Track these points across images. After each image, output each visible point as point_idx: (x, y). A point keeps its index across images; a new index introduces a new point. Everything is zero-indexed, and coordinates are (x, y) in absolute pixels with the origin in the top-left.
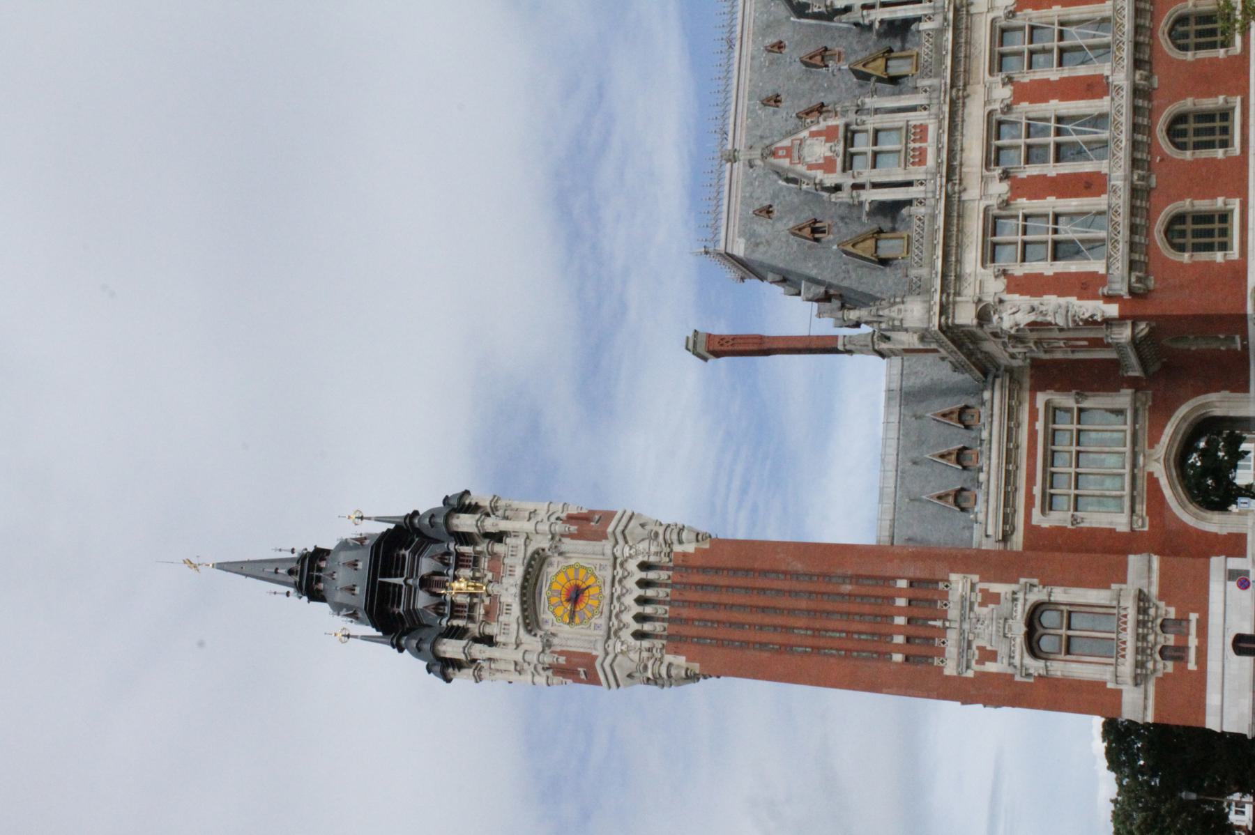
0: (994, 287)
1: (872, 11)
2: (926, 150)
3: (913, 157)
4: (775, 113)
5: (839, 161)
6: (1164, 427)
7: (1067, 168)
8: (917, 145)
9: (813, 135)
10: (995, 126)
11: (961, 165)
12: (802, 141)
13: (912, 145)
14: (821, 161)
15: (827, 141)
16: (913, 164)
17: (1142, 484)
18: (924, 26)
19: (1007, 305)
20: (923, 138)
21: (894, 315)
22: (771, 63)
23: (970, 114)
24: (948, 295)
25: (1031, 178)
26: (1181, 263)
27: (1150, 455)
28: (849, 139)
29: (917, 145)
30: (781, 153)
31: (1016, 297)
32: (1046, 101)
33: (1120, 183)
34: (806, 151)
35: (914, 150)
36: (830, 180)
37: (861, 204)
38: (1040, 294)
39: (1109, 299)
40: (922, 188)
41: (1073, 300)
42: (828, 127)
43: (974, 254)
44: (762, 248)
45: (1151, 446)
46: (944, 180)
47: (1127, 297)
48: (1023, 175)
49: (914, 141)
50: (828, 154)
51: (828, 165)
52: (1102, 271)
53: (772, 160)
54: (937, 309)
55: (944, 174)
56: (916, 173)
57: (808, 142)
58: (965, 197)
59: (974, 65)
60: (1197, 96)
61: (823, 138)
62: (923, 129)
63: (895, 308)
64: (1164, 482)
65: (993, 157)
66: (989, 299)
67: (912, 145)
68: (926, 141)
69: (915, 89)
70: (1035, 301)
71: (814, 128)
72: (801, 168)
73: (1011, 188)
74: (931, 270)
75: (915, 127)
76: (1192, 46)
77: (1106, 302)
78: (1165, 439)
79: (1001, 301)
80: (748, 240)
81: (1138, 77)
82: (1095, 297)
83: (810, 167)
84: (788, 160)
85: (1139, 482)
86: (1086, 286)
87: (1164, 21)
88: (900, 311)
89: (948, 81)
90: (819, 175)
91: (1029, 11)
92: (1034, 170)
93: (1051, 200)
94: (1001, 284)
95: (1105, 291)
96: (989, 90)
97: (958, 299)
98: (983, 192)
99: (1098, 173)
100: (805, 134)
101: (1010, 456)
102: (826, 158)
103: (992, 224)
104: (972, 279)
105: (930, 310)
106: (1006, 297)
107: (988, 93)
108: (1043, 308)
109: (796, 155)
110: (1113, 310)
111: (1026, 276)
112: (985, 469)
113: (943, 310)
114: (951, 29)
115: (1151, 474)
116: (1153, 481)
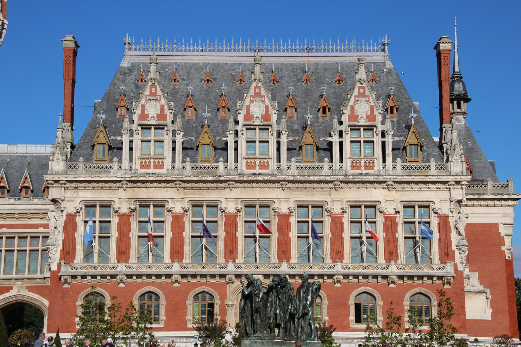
0: (70, 208)
1: (233, 135)
2: (150, 169)
3: (145, 162)
4: (201, 80)
5: (146, 122)
6: (37, 293)
7: (134, 242)
8: (152, 164)
9: (162, 107)
10: (160, 205)
11: (139, 188)
12: (159, 101)
13: (152, 161)
14: (146, 112)
15: (158, 115)
16: (142, 162)
17: (6, 284)
18: (221, 165)
19: (60, 213)
20: (156, 167)
21: (56, 156)
22: (233, 77)
23: (166, 191)
24: (65, 184)
25: (130, 224)
26: (77, 300)
27: (22, 287)
28: (158, 127)
29: (152, 164)
30: (153, 90)
31: (64, 218)
32: (172, 230)
33: (119, 269)
34: (153, 103)
35: (150, 162)
36: (136, 117)
37: (121, 135)
38: (65, 230)
39: (59, 265)
40: (127, 167)
41: (61, 247)
42: (166, 115)
43: (89, 196)
44: (121, 77)
45: (27, 288)
46: (128, 179)
47: (60, 274)
48: (131, 219)
49: (155, 162)
50: (150, 116)
51: (144, 116)
52: (75, 261)
53: (150, 84)
54: (56, 178)
55: (131, 179)
56: (136, 165)
57: (158, 104)
58: (121, 190)
59: (197, 192)
60: (166, 306)
61: (159, 113)
62: (162, 167)
63: (60, 156)
64: (7, 295)
65: (144, 205)
66: (63, 205)
67: (152, 161)
68: (154, 168)
69: (183, 161)
70: (61, 228)
71: (166, 107)
72: (143, 101)
73: (124, 215)
74: (81, 173)
75: (163, 162)
76: (157, 303)
77: (58, 264)
78: (31, 294)
79: (62, 211)
80: (128, 68)
81: (176, 276)
82: (60, 260)
83: (143, 107)
84: (148, 93)
85: (7, 282)
86: (68, 255)
87: (210, 289)
88: (58, 159)
89: (184, 179)
90: (138, 112)
91: (224, 220)
92: (134, 225)
93: (117, 235)
94: (72, 211)
95: (63, 264)
96: (182, 200)
97: (63, 189)
98: (122, 200)
99: (129, 258)
100: (163, 102)
101: (23, 214)
102: (148, 115)
103: (106, 206)
104: (75, 195)
105: (57, 173)
106: (64, 213)
107: (177, 201)
108: (56, 232)
109: (151, 98)
110: (54, 268)
111: (76, 223)
112: (19, 202)
113: (57, 181)
114: (215, 179)
115: (11, 288)
116: (8, 289)
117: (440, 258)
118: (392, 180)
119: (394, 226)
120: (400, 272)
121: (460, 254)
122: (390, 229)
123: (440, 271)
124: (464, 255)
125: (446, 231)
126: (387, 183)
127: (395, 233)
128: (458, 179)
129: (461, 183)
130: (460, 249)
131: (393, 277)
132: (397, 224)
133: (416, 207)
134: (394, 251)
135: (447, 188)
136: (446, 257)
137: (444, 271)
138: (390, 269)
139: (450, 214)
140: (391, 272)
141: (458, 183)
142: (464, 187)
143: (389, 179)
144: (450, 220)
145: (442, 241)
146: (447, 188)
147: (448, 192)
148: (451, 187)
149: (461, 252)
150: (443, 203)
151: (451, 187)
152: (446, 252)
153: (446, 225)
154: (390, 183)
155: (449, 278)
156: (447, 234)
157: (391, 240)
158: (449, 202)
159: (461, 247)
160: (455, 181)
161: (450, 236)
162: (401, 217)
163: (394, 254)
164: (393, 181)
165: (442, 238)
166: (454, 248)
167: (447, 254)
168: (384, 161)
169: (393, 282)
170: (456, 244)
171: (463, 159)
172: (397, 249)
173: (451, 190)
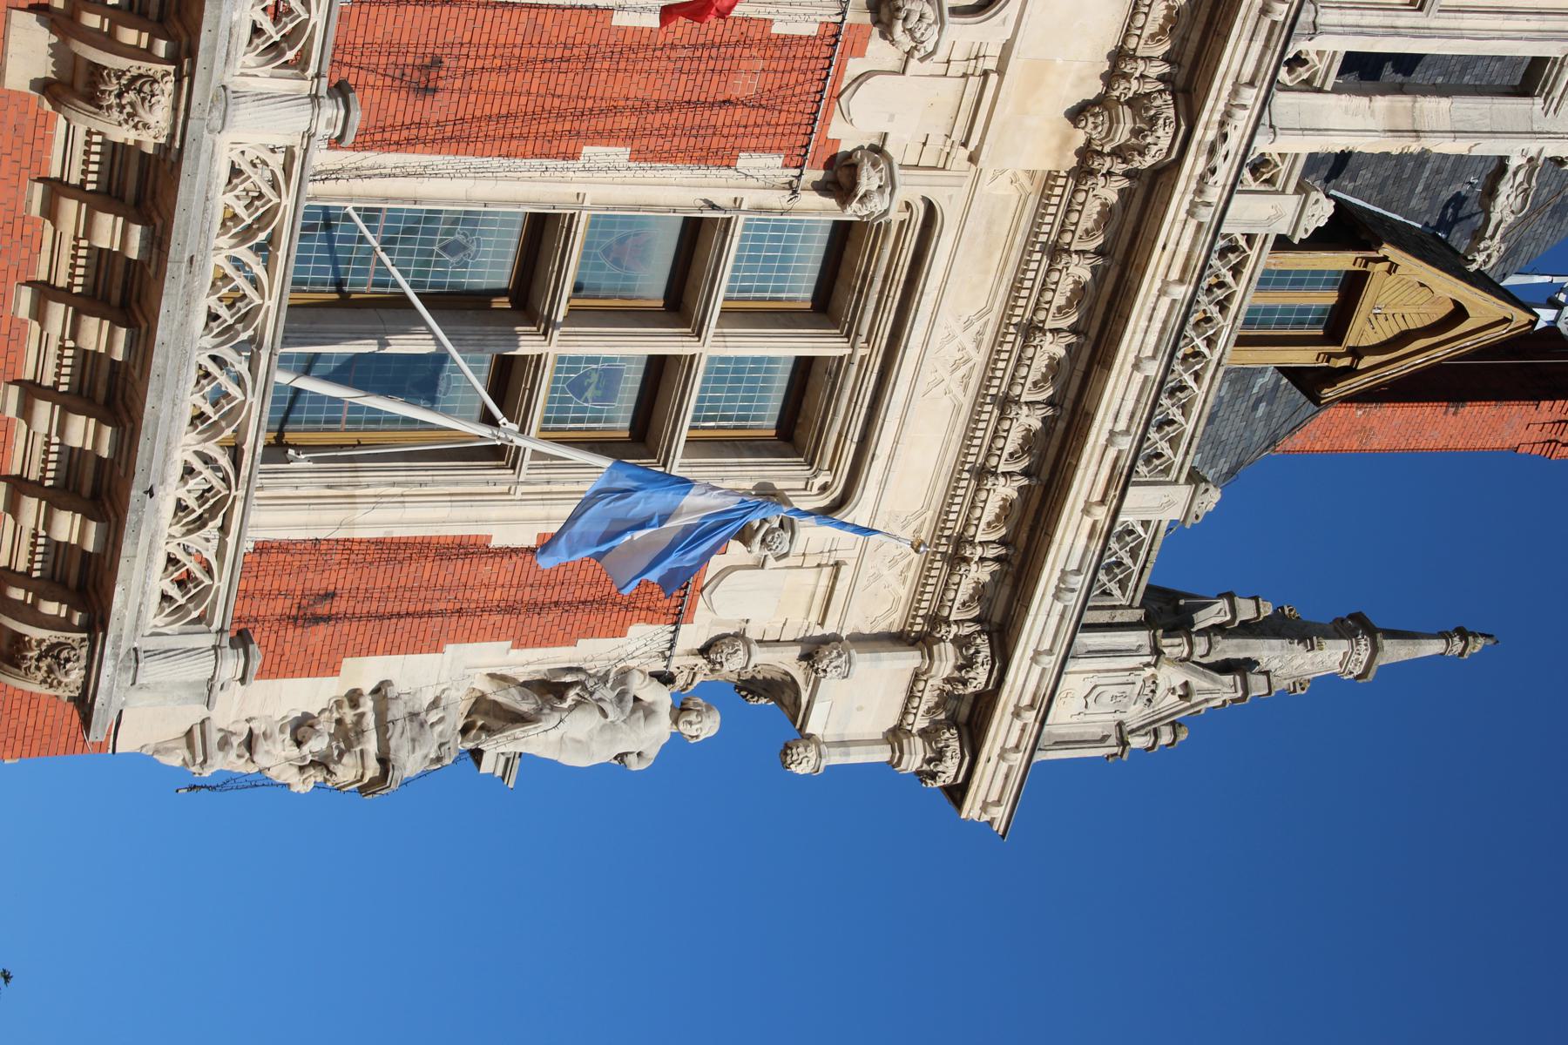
117: (284, 547)
118: (1194, 164)
119: (695, 132)
120: (206, 200)
121: (301, 728)
122: (681, 87)
123: (160, 582)
124: (278, 759)
125: (537, 608)
126: (1165, 106)
127: (629, 137)
128: (1002, 730)
129: (951, 741)
130: (347, 736)
131: (159, 116)
132: (725, 159)
133: (824, 346)
134: (439, 108)
135: (935, 620)
136: (280, 606)
137: (154, 619)
138: (267, 80)
139: (693, 635)
140: (226, 97)
141: (969, 718)
142: (914, 759)
143: (1205, 132)
144: (641, 642)
145: (458, 569)
146: (935, 620)
147: (892, 620)
148: (946, 661)
149: (317, 745)
150: (813, 582)
151: (946, 661)
152: (340, 606)
153: (600, 603)
154: (1162, 140)
155: (76, 675)
156: (510, 609)
157: (567, 84)
158: (802, 623)
159: (371, 745)
160: (985, 703)
161: (496, 636)
162: (778, 199)
163: (400, 107)
164: (1166, 173)
165: (486, 570)
166: (364, 672)
167: (308, 614)
168: (1363, 71)
169: (72, 85)
170: (400, 686)
171: (1137, 742)
172: (455, 137)
173: (910, 660)
